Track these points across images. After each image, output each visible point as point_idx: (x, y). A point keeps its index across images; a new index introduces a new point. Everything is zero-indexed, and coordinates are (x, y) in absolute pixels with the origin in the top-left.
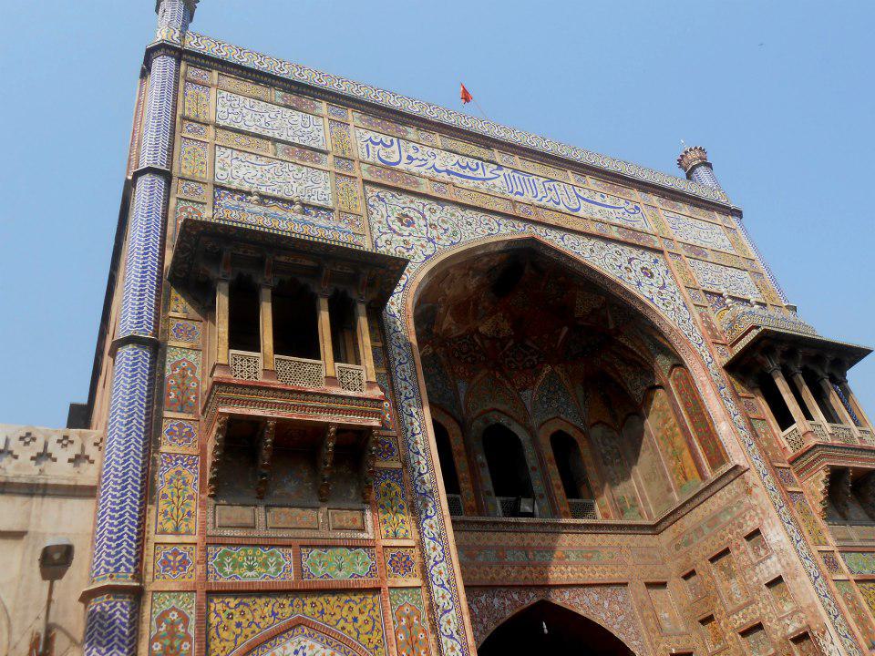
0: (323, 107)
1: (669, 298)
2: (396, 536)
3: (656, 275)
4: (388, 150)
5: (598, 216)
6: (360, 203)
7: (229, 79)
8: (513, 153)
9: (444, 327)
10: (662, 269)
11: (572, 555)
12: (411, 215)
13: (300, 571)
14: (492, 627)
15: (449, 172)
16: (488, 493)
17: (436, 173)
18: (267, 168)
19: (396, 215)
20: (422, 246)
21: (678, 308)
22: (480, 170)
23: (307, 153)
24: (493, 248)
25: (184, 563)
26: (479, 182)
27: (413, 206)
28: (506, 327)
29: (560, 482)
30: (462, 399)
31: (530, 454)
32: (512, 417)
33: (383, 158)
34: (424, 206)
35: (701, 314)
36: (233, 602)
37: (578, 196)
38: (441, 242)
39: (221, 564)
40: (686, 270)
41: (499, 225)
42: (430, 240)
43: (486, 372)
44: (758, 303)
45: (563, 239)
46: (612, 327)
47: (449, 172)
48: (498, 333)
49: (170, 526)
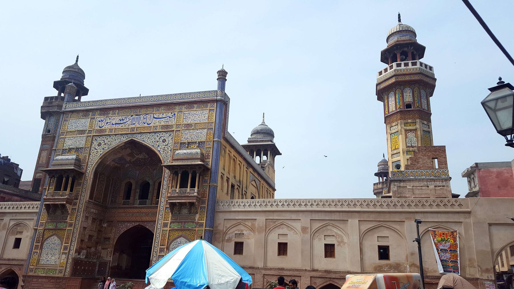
0: (91, 113)
1: (167, 149)
2: (71, 221)
3: (167, 141)
4: (102, 122)
5: (157, 124)
6: (90, 144)
7: (73, 115)
8: (137, 108)
9: (129, 159)
10: (170, 138)
11: (150, 214)
12: (101, 142)
13: (56, 226)
14: (126, 230)
15: (116, 124)
16: (136, 199)
17: (112, 126)
18: (73, 140)
19: (98, 144)
20: (101, 151)
21: (168, 151)
22: (125, 120)
23: (82, 132)
24: (121, 145)
25: (43, 225)
26: (123, 124)
27: (103, 139)
28: (147, 157)
29: (156, 195)
30: (137, 175)
31: (151, 188)
32: (150, 178)
33: (100, 126)
34: (106, 138)
36: (48, 231)
37: (154, 117)
38: (106, 149)
39: (47, 225)
40: (179, 136)
41: (124, 137)
42: (103, 149)
43: (146, 166)
45: (141, 137)
47: (116, 124)
48: (145, 157)
49: (42, 220)
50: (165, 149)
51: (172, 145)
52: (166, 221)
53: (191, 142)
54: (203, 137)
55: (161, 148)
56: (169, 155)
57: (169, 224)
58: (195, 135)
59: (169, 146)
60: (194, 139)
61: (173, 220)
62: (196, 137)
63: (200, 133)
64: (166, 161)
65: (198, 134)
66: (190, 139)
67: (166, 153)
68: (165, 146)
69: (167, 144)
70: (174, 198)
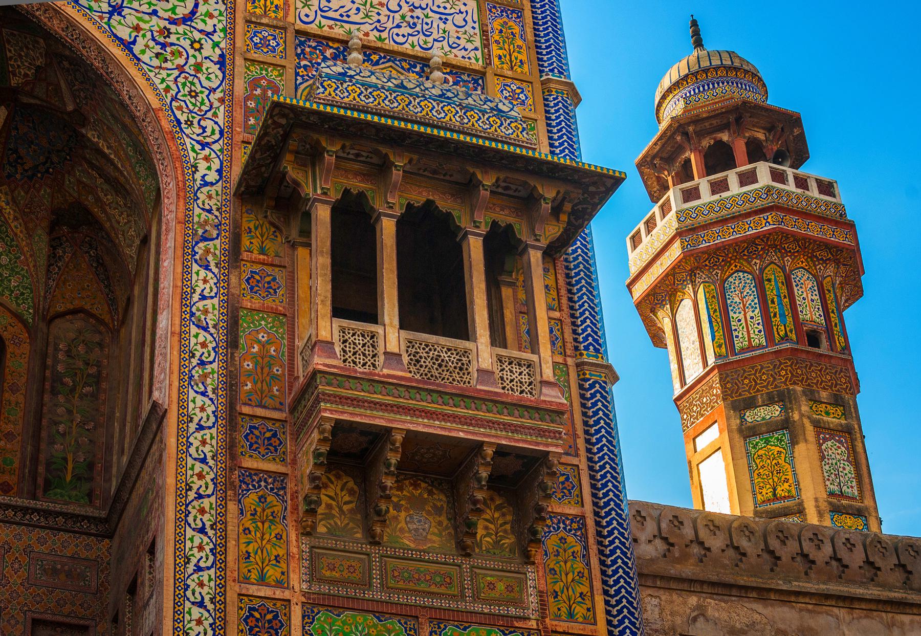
1: (186, 44)
21: (198, 67)
35: (254, 83)
44: (454, 70)
46: (70, 108)
50: (173, 38)
51: (224, 30)
52: (262, 580)
53: (376, 50)
54: (462, 42)
55: (137, 28)
56: (214, 90)
57: (297, 613)
58: (403, 17)
59: (208, 34)
60: (400, 39)
61: (325, 589)
62: (411, 31)
63: (431, 14)
64: (190, 123)
65: (418, 12)
66: (367, 28)
67: (181, 68)
68: (173, 22)
69: (181, 12)
70: (377, 397)
